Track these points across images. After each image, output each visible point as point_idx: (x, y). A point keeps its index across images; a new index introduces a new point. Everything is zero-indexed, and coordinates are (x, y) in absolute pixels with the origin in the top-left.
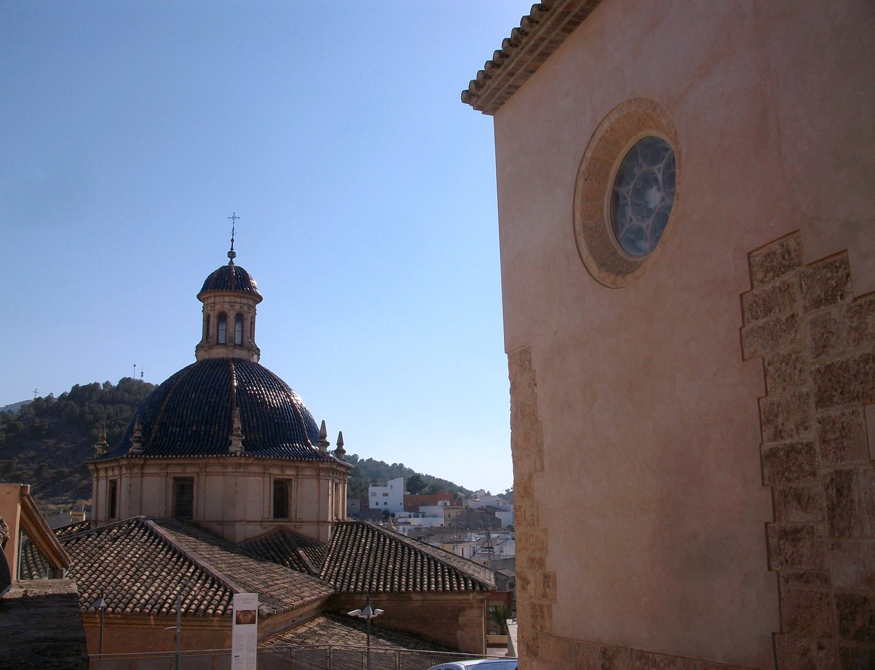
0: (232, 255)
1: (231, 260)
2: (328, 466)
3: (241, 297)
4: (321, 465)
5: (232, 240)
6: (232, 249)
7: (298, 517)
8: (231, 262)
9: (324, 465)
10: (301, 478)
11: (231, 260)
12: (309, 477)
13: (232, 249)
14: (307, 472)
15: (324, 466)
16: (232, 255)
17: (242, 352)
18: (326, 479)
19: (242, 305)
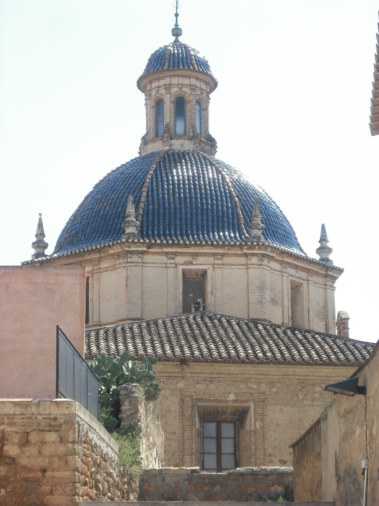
0: (177, 32)
1: (177, 38)
2: (120, 250)
3: (158, 79)
4: (112, 252)
5: (177, 15)
6: (176, 25)
7: (95, 321)
8: (176, 41)
9: (114, 249)
10: (96, 273)
11: (177, 38)
12: (107, 269)
13: (176, 25)
14: (105, 264)
15: (115, 252)
16: (177, 32)
17: (155, 143)
18: (124, 267)
19: (157, 89)
